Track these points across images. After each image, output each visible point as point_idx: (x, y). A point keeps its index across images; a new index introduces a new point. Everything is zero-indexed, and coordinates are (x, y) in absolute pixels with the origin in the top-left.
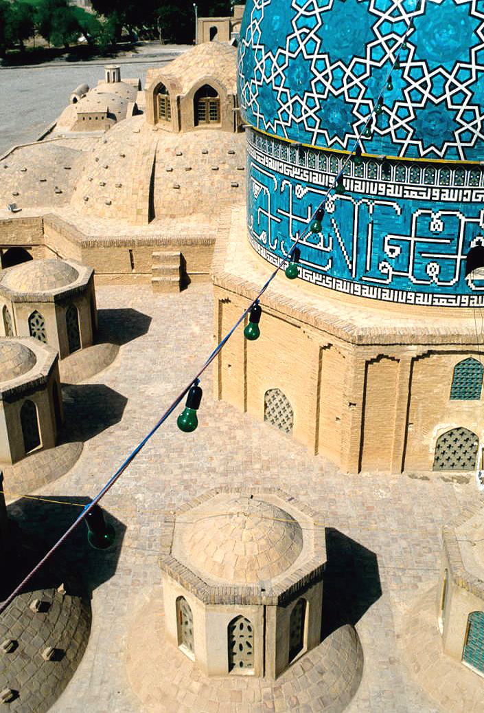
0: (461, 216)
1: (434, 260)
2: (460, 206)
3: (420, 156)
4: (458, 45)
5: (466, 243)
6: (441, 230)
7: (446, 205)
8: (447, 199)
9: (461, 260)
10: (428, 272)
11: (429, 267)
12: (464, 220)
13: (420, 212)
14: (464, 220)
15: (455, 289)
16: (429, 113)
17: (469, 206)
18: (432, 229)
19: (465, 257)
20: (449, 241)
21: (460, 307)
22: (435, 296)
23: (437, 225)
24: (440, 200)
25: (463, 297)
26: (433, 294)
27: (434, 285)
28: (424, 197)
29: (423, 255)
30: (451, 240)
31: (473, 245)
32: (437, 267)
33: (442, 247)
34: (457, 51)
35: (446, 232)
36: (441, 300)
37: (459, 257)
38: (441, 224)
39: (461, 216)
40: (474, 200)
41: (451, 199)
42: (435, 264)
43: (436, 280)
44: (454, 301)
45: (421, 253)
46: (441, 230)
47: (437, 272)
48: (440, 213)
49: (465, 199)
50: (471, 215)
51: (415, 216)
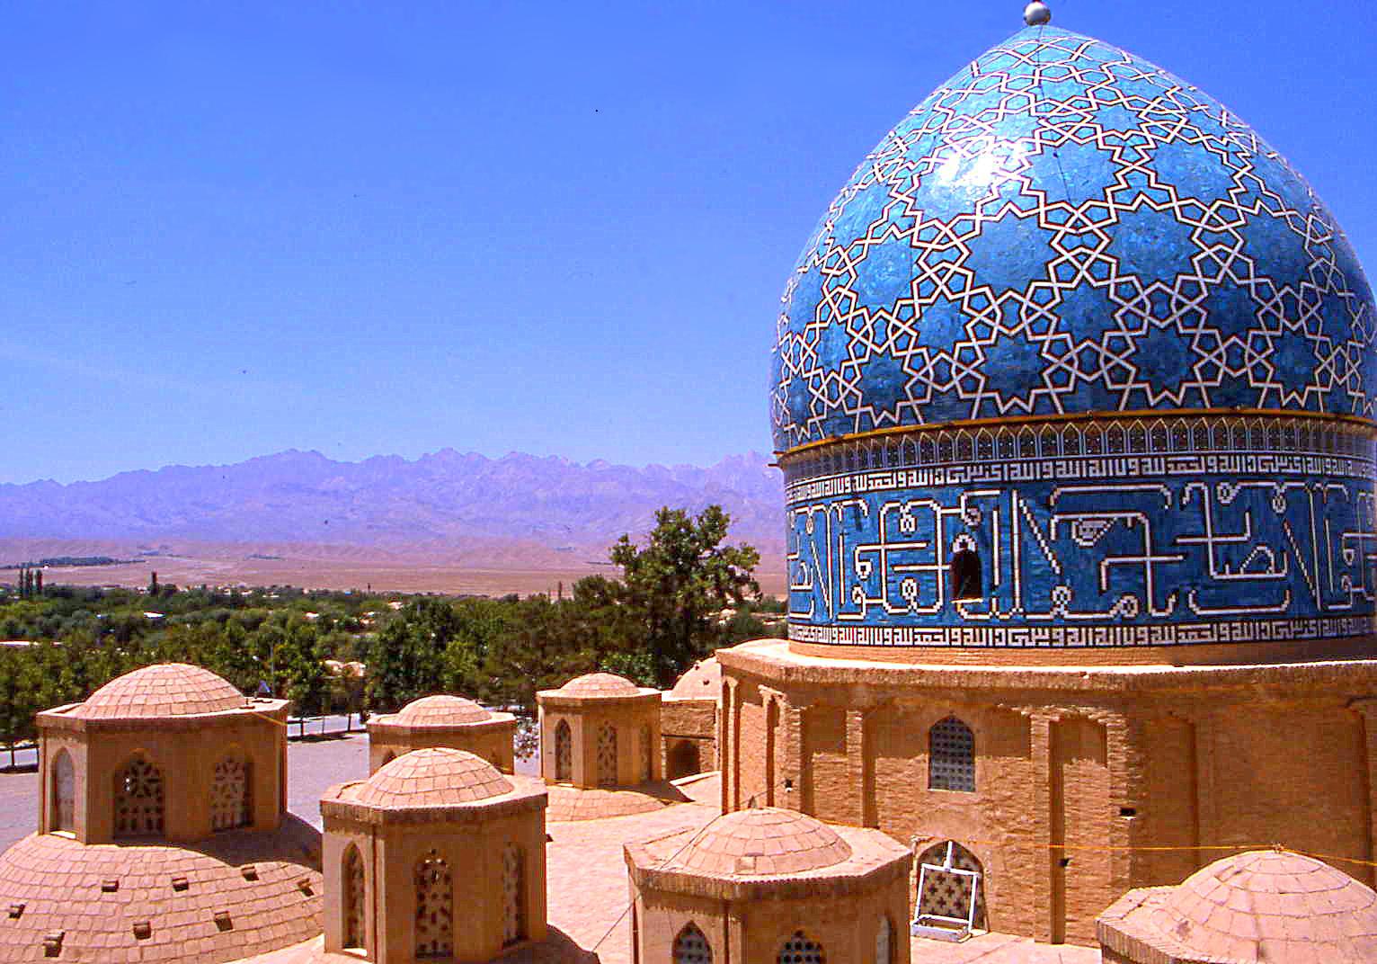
0: (935, 507)
1: (910, 575)
2: (932, 492)
3: (874, 428)
4: (898, 280)
5: (947, 547)
6: (912, 529)
7: (917, 493)
8: (915, 484)
9: (944, 571)
10: (904, 594)
11: (904, 585)
12: (940, 512)
13: (888, 506)
14: (940, 512)
15: (941, 619)
16: (875, 368)
17: (944, 490)
18: (903, 530)
19: (947, 567)
20: (924, 545)
21: (950, 646)
22: (916, 630)
23: (908, 523)
24: (907, 487)
25: (954, 630)
26: (914, 627)
27: (912, 614)
28: (890, 486)
29: (896, 569)
30: (928, 542)
31: (957, 549)
32: (914, 585)
33: (916, 554)
34: (898, 286)
35: (920, 531)
36: (925, 637)
37: (940, 568)
38: (912, 520)
39: (935, 507)
40: (949, 481)
41: (921, 483)
42: (911, 581)
43: (915, 605)
44: (941, 637)
45: (892, 566)
46: (912, 529)
47: (914, 594)
48: (910, 504)
49: (937, 482)
50: (948, 504)
51: (883, 512)
